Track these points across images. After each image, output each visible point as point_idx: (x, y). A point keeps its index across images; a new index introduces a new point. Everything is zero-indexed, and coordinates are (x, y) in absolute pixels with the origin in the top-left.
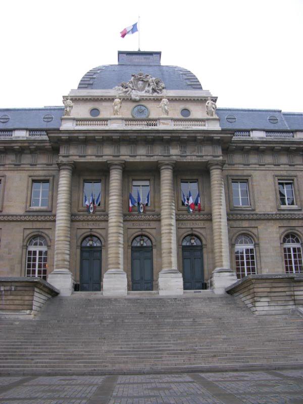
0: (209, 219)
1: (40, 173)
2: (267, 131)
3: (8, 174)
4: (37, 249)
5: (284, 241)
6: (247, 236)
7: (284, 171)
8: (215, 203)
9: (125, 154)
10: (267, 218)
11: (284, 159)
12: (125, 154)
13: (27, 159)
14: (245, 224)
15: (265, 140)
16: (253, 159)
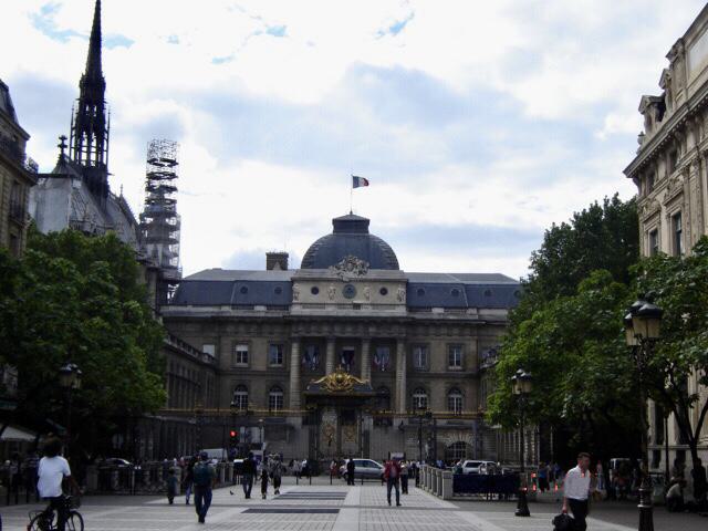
0: (394, 375)
1: (276, 338)
2: (445, 308)
3: (253, 340)
4: (276, 394)
5: (450, 393)
6: (423, 390)
7: (455, 339)
8: (398, 367)
9: (337, 331)
10: (437, 376)
11: (456, 331)
12: (337, 331)
13: (266, 329)
14: (421, 380)
15: (442, 317)
16: (432, 331)
